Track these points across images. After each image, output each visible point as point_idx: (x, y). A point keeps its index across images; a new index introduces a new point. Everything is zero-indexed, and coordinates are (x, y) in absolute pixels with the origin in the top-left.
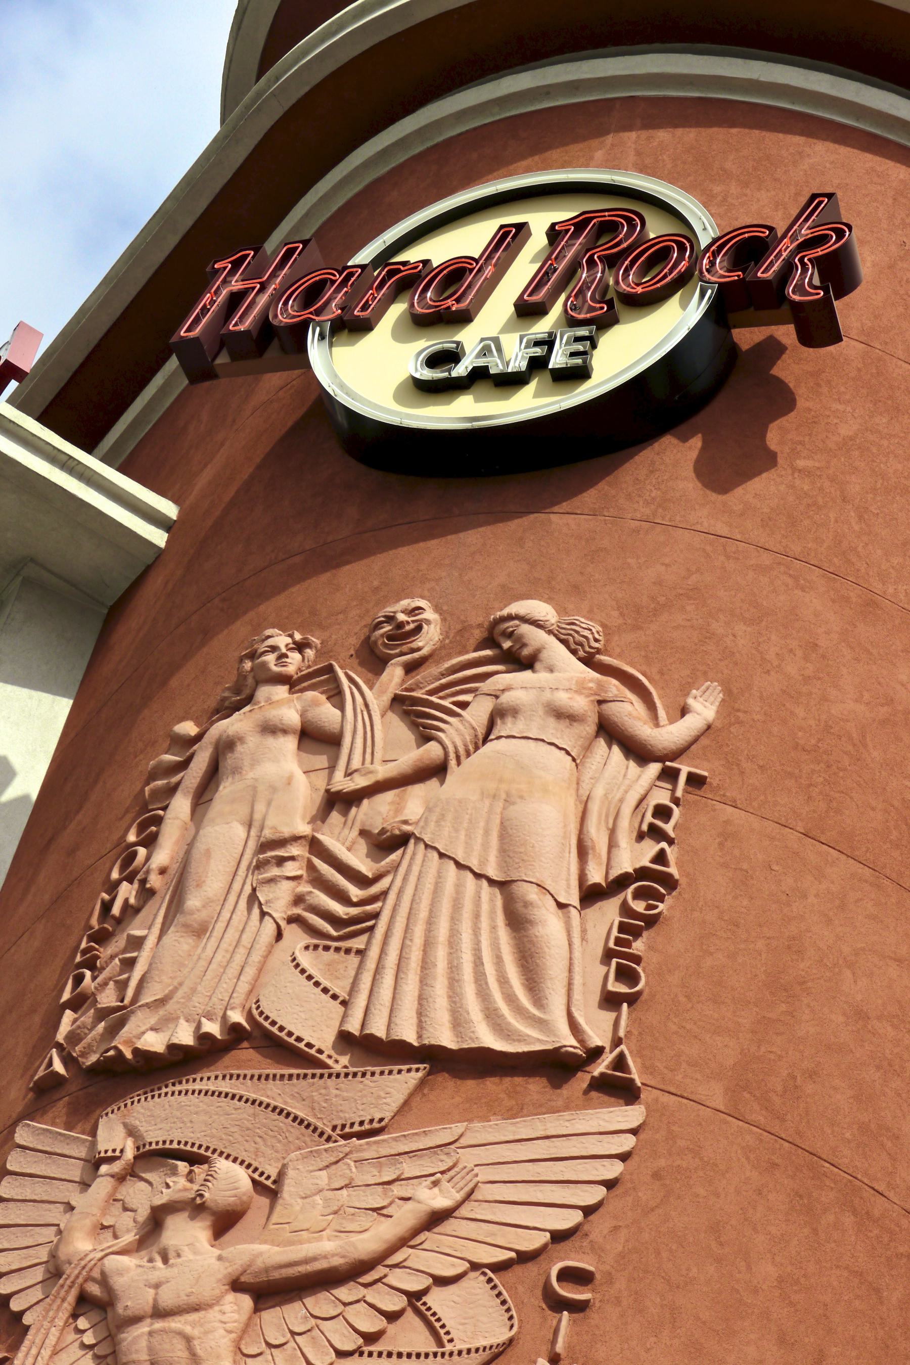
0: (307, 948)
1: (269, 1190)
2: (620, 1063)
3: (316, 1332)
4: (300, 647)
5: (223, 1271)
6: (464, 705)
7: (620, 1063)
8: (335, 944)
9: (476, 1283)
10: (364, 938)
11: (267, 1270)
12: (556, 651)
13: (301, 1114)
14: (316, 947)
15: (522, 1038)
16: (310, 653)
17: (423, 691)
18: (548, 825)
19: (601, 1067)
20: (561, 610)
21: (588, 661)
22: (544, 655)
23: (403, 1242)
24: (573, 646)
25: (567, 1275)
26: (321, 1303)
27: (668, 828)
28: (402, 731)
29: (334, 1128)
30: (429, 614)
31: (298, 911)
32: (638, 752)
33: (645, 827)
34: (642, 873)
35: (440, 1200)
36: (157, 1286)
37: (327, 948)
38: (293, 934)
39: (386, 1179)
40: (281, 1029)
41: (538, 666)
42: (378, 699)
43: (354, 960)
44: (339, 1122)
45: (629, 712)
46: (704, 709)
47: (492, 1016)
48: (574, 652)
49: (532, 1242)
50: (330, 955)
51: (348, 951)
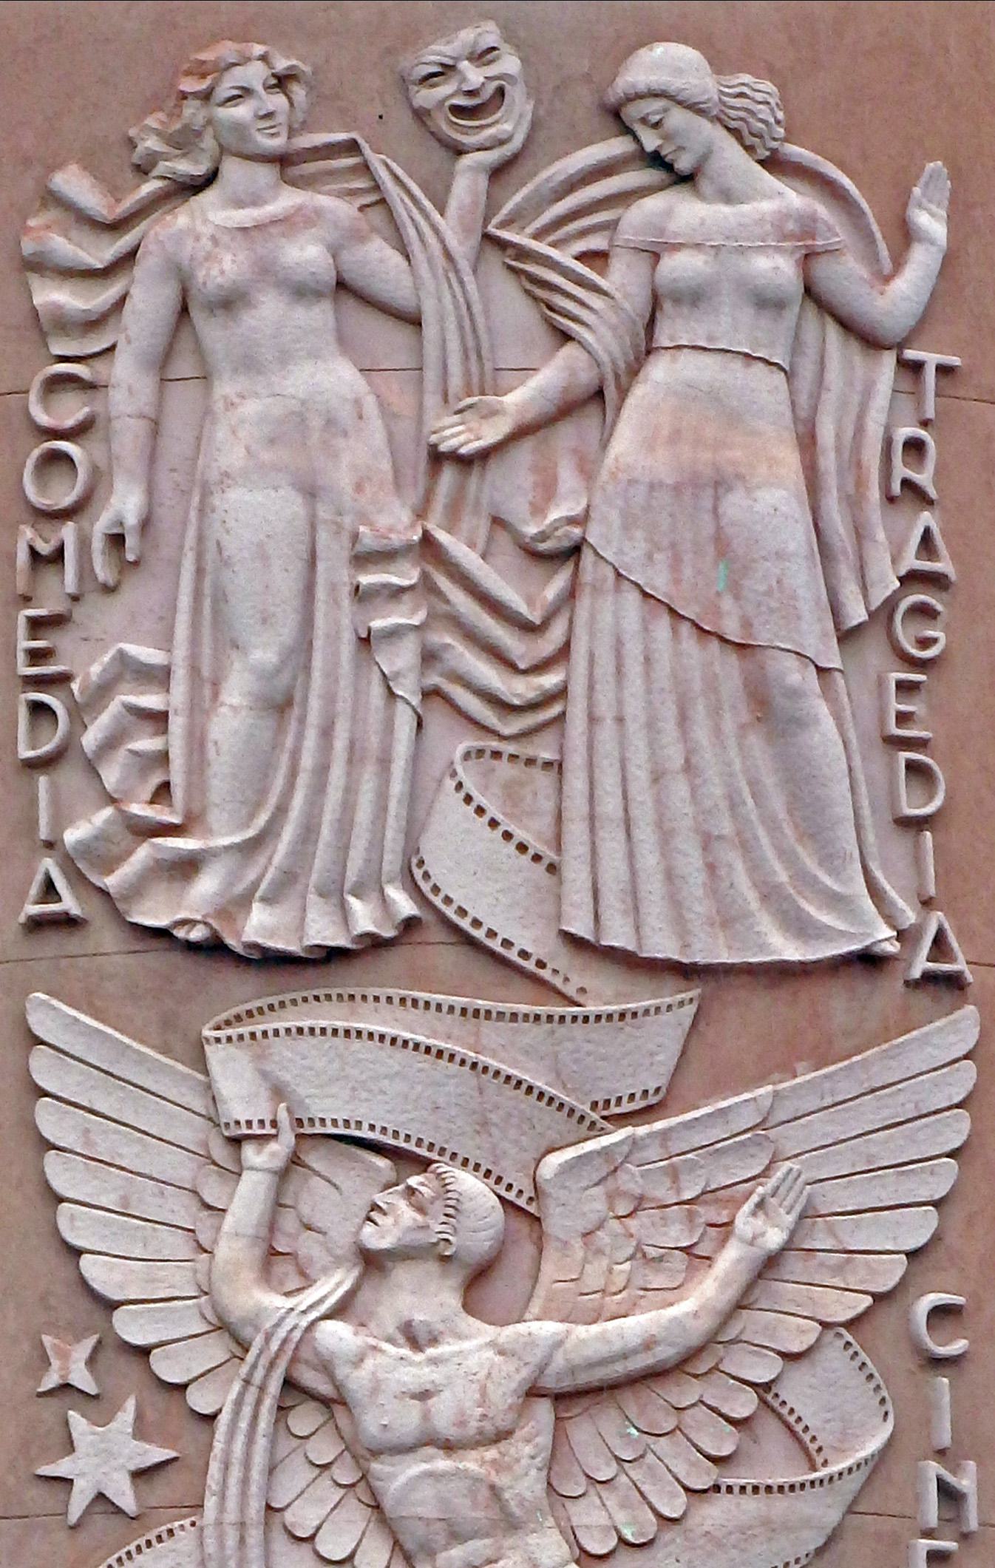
0: (467, 756)
1: (524, 1214)
2: (940, 946)
3: (650, 1458)
4: (282, 82)
5: (511, 1378)
6: (596, 258)
7: (940, 946)
8: (509, 748)
9: (834, 1357)
10: (549, 737)
11: (573, 1370)
12: (732, 159)
13: (540, 1084)
14: (480, 752)
15: (822, 933)
16: (299, 92)
17: (530, 229)
18: (771, 505)
19: (921, 965)
20: (719, 64)
21: (773, 163)
22: (713, 166)
23: (740, 1305)
24: (750, 140)
25: (940, 1313)
26: (653, 1407)
27: (924, 478)
28: (510, 307)
29: (594, 1105)
30: (509, 64)
31: (435, 679)
32: (867, 338)
33: (896, 488)
34: (911, 579)
35: (775, 1238)
36: (424, 1395)
37: (497, 755)
38: (438, 721)
39: (688, 1195)
40: (477, 923)
41: (705, 185)
42: (454, 228)
43: (543, 781)
44: (600, 1097)
45: (847, 275)
46: (931, 222)
47: (770, 894)
48: (749, 149)
49: (890, 1273)
50: (504, 769)
51: (530, 762)
